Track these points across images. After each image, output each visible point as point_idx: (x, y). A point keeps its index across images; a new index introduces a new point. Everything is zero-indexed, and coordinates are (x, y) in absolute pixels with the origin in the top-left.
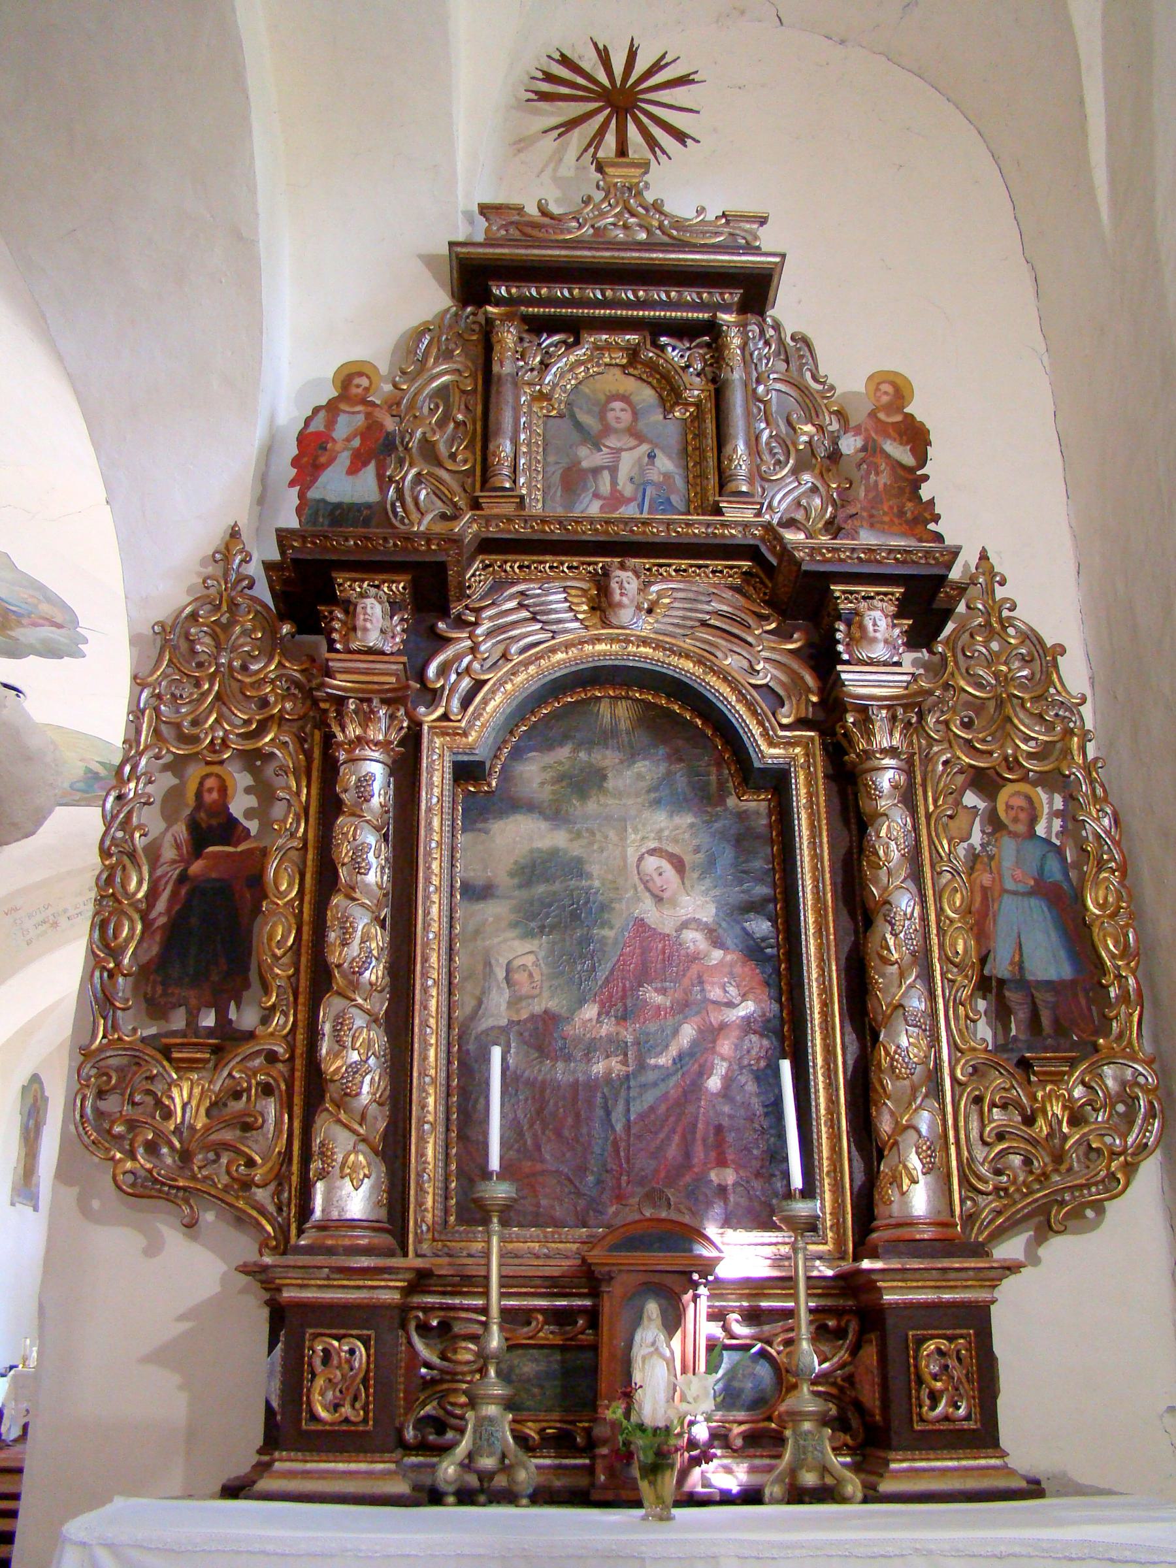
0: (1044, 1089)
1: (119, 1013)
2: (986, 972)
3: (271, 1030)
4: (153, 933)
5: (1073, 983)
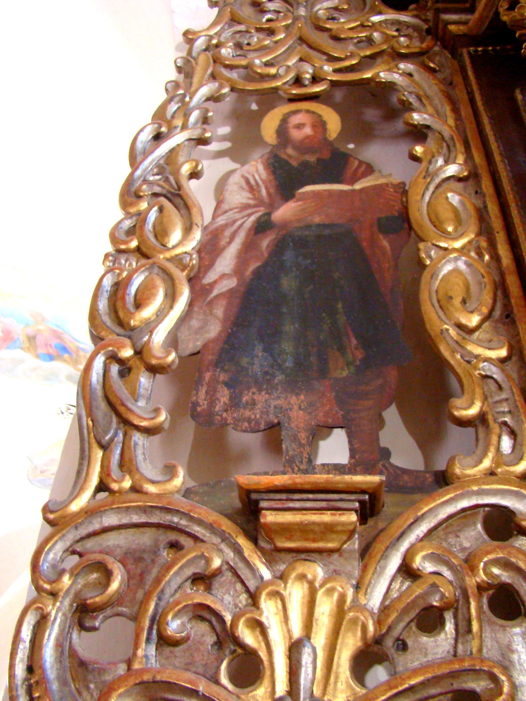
1: (137, 437)
3: (487, 463)
4: (211, 304)
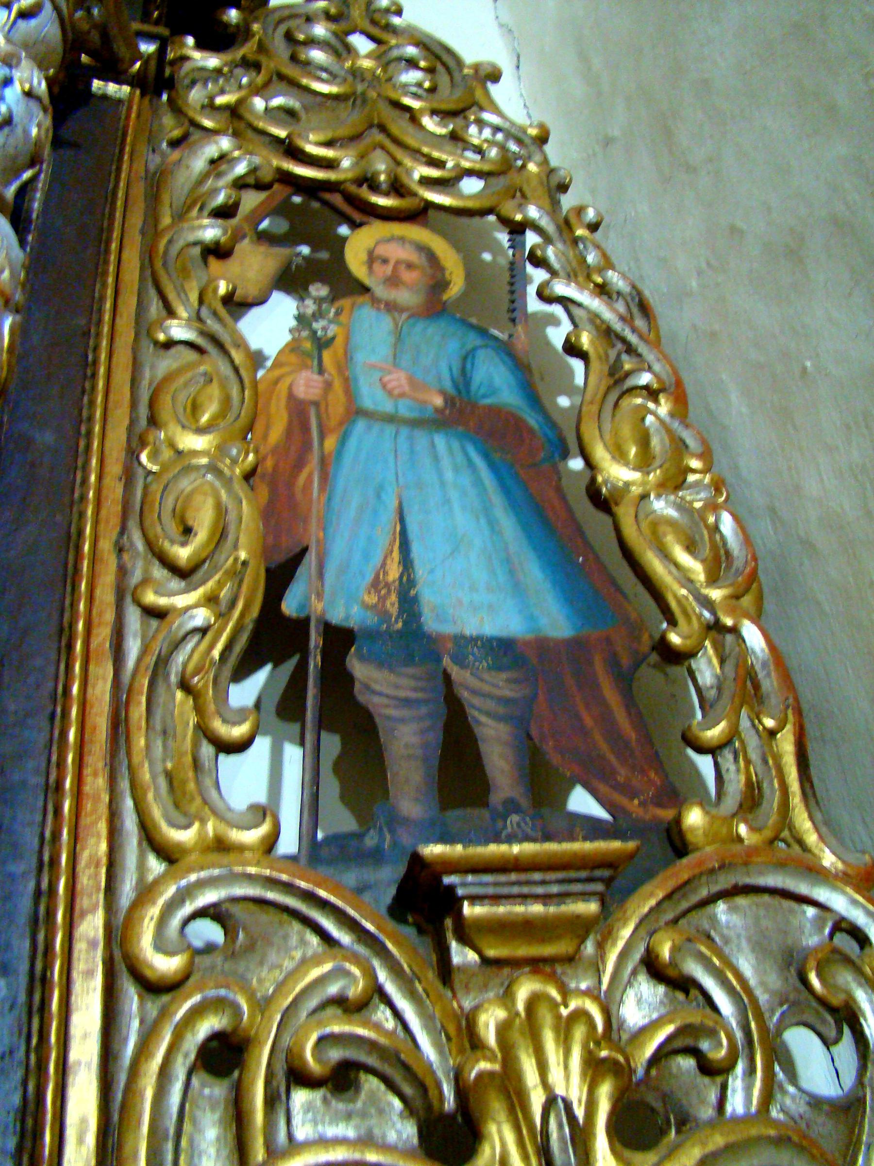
0: (507, 997)
2: (290, 606)
5: (577, 649)
